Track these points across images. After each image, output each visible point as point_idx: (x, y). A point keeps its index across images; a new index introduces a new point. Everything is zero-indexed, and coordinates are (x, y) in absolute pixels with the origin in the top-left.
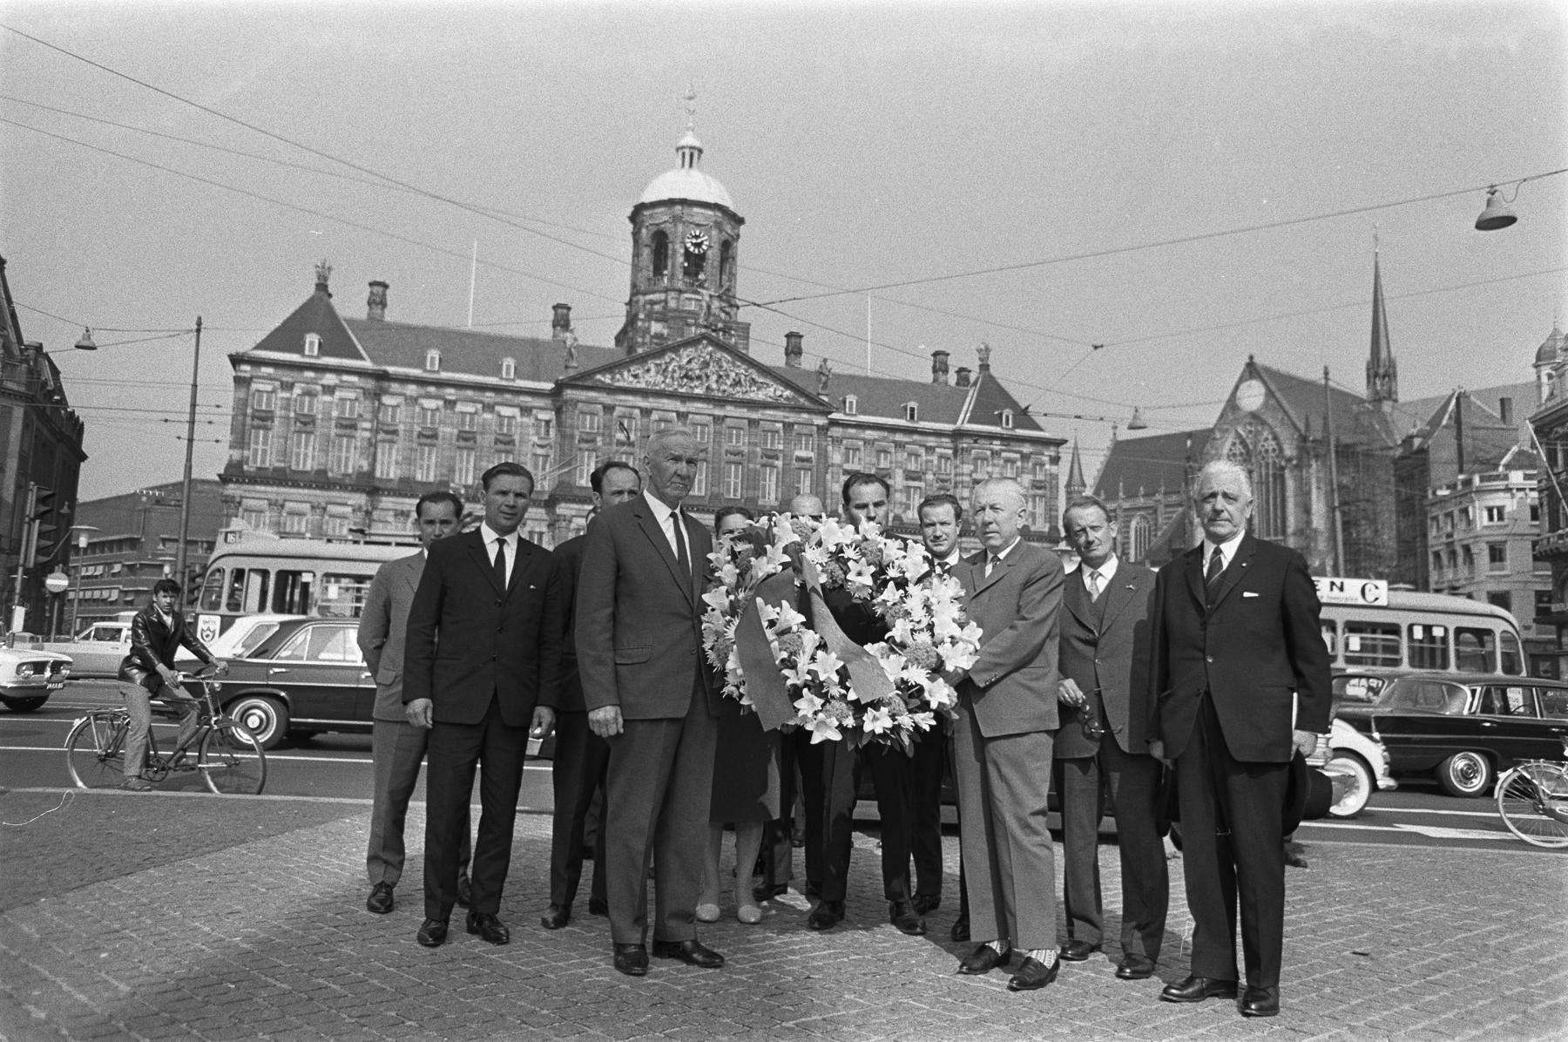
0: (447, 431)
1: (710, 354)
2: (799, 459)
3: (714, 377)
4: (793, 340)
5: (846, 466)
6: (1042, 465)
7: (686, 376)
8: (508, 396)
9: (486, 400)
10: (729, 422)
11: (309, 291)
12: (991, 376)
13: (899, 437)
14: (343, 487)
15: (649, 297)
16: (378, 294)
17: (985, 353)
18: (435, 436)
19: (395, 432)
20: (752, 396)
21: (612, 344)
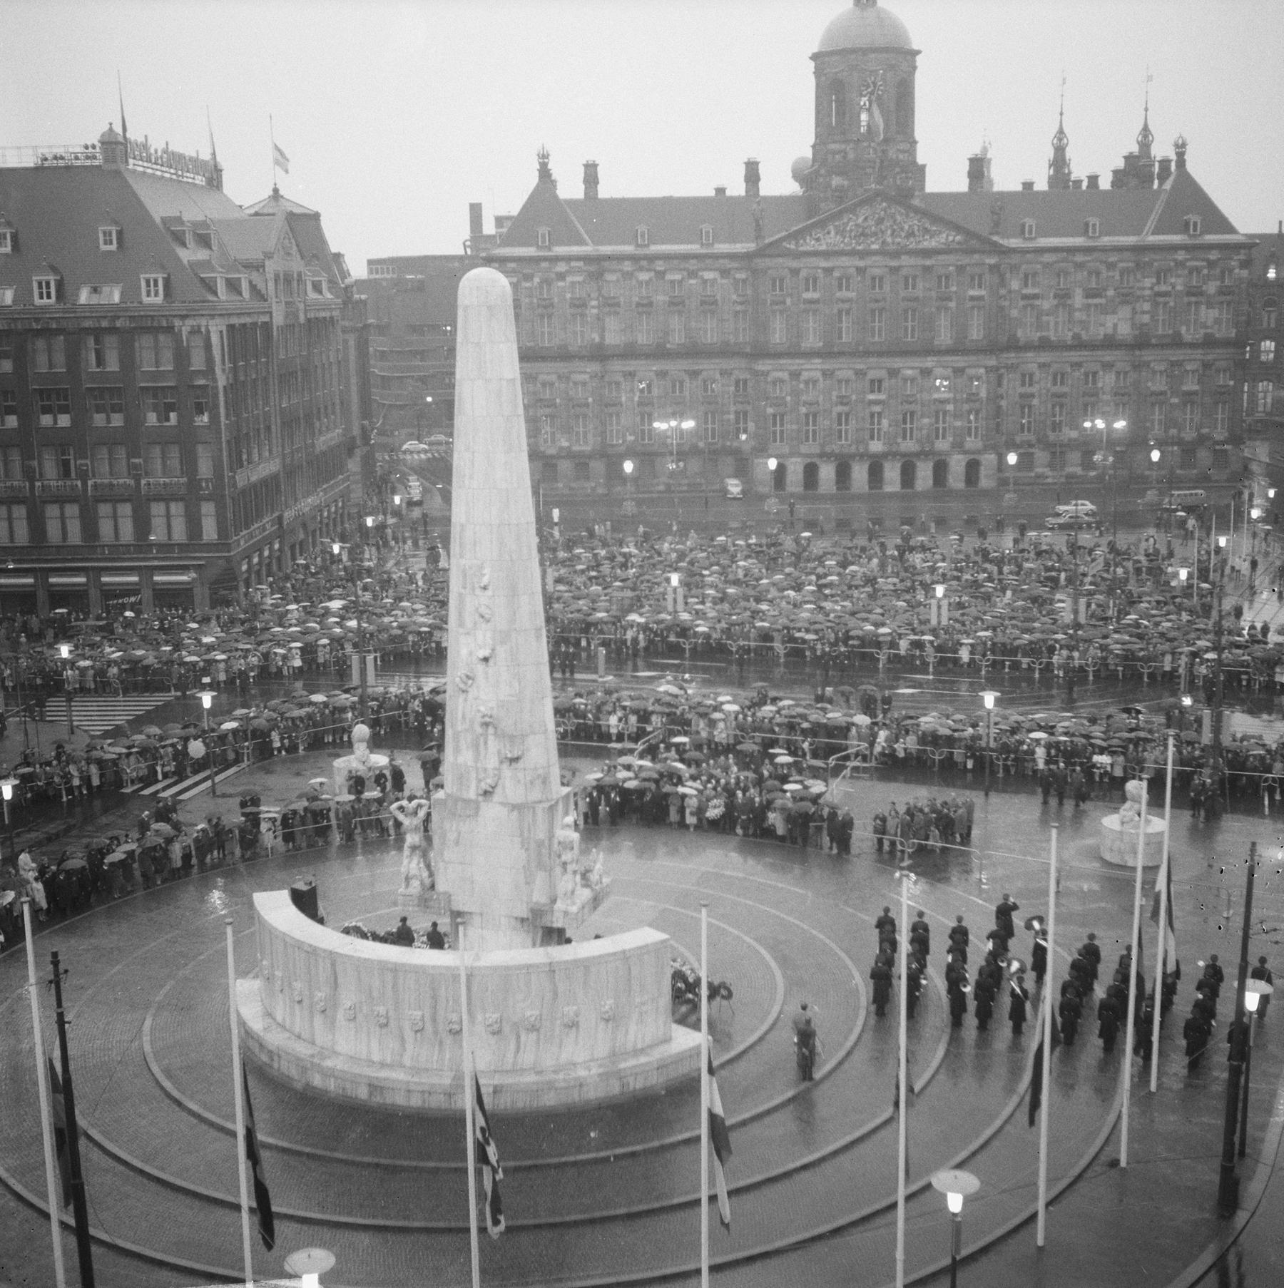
0: (661, 298)
1: (885, 210)
2: (972, 298)
3: (889, 232)
5: (1024, 291)
6: (1231, 271)
7: (862, 234)
8: (708, 261)
11: (533, 180)
12: (1188, 176)
13: (1079, 258)
14: (581, 358)
16: (591, 175)
17: (1181, 148)
18: (651, 304)
19: (618, 305)
20: (926, 244)
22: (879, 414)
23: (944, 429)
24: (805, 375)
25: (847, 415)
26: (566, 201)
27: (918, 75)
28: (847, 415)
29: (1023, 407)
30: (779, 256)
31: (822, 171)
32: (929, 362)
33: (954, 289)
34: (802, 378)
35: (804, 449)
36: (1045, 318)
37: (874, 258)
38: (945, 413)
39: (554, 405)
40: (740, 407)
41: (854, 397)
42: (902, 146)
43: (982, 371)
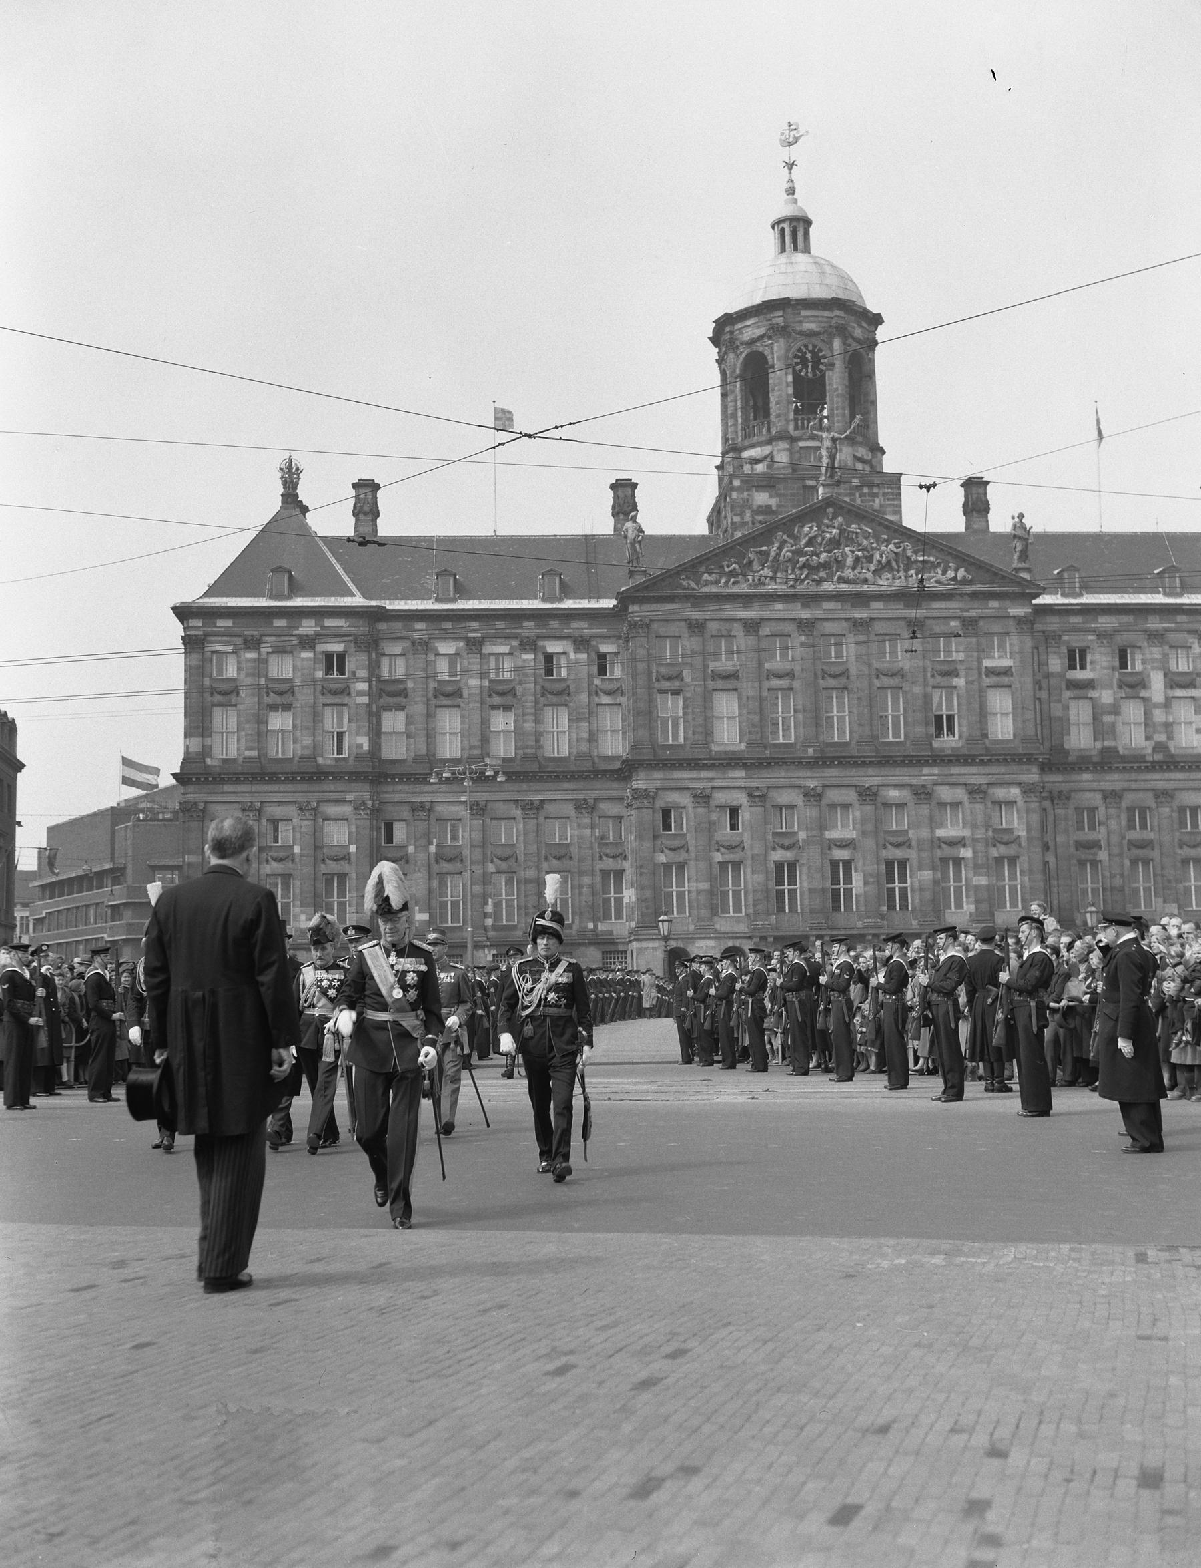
2: (991, 672)
4: (974, 490)
8: (555, 624)
9: (526, 633)
10: (879, 627)
11: (272, 504)
13: (1154, 624)
15: (745, 454)
18: (457, 693)
21: (702, 529)
22: (848, 865)
23: (958, 890)
24: (720, 797)
25: (792, 866)
26: (326, 539)
27: (881, 357)
28: (792, 866)
29: (1082, 864)
30: (671, 599)
31: (736, 483)
32: (928, 775)
33: (961, 656)
34: (713, 803)
35: (721, 925)
36: (1107, 719)
37: (826, 605)
38: (958, 862)
39: (291, 857)
40: (609, 864)
41: (802, 835)
42: (862, 452)
43: (1015, 792)
